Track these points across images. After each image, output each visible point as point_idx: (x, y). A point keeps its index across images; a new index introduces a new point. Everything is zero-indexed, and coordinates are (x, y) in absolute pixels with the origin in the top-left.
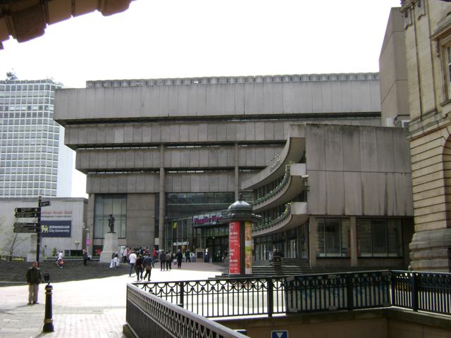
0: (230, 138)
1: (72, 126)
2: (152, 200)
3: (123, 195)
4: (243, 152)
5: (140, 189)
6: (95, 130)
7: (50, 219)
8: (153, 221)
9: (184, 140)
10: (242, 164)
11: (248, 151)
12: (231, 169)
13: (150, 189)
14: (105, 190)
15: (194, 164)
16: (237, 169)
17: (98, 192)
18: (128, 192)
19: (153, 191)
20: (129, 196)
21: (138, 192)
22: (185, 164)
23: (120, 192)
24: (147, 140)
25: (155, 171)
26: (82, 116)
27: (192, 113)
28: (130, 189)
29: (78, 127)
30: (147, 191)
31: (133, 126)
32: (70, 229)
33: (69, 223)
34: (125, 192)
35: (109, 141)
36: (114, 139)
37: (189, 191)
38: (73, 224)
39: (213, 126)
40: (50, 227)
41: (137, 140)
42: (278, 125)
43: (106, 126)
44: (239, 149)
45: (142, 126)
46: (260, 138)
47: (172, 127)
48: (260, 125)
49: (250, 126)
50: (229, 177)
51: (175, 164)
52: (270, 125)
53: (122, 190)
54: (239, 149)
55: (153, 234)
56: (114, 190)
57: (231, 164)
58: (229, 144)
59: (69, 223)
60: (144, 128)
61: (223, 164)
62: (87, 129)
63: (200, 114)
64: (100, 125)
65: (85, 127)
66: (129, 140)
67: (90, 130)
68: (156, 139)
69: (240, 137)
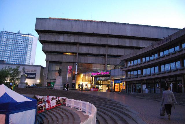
0: (105, 43)
4: (109, 49)
7: (28, 72)
9: (87, 42)
10: (109, 54)
12: (104, 56)
14: (53, 60)
15: (90, 52)
16: (107, 56)
17: (50, 60)
19: (73, 62)
20: (63, 63)
22: (87, 52)
24: (72, 41)
26: (47, 29)
27: (92, 32)
28: (64, 60)
30: (70, 61)
31: (67, 35)
32: (35, 76)
33: (35, 74)
34: (62, 61)
35: (57, 40)
37: (87, 63)
38: (37, 74)
39: (99, 38)
40: (28, 75)
41: (69, 40)
42: (123, 40)
45: (71, 35)
46: (117, 44)
47: (83, 37)
48: (117, 39)
49: (113, 39)
52: (120, 40)
53: (60, 60)
56: (57, 60)
57: (105, 53)
58: (103, 46)
59: (35, 74)
61: (102, 53)
62: (48, 35)
63: (95, 32)
65: (47, 34)
66: (65, 40)
67: (49, 35)
68: (76, 41)
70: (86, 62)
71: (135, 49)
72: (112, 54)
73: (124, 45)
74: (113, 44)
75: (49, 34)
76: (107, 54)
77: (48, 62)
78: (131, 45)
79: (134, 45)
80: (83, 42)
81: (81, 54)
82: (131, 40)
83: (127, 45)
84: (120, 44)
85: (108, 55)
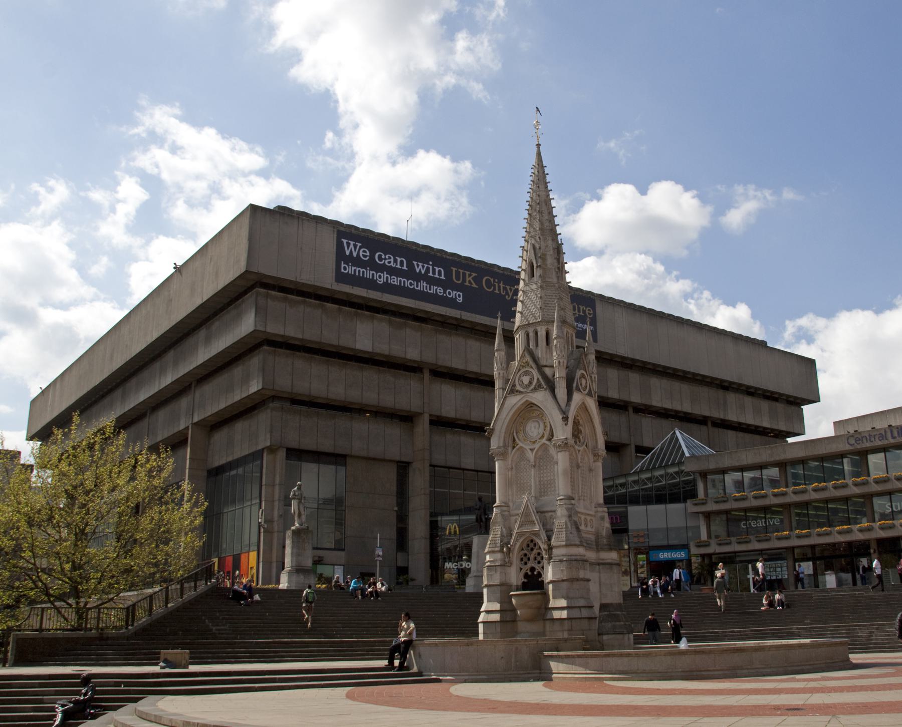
1: (273, 293)
2: (390, 475)
3: (337, 458)
8: (393, 519)
13: (395, 453)
14: (308, 443)
17: (294, 445)
19: (398, 459)
20: (349, 460)
23: (337, 452)
24: (413, 354)
25: (407, 419)
28: (357, 447)
35: (345, 341)
51: (448, 411)
55: (394, 546)
56: (326, 446)
68: (429, 357)
70: (452, 461)
77: (282, 454)
78: (625, 397)
80: (457, 363)
81: (440, 423)
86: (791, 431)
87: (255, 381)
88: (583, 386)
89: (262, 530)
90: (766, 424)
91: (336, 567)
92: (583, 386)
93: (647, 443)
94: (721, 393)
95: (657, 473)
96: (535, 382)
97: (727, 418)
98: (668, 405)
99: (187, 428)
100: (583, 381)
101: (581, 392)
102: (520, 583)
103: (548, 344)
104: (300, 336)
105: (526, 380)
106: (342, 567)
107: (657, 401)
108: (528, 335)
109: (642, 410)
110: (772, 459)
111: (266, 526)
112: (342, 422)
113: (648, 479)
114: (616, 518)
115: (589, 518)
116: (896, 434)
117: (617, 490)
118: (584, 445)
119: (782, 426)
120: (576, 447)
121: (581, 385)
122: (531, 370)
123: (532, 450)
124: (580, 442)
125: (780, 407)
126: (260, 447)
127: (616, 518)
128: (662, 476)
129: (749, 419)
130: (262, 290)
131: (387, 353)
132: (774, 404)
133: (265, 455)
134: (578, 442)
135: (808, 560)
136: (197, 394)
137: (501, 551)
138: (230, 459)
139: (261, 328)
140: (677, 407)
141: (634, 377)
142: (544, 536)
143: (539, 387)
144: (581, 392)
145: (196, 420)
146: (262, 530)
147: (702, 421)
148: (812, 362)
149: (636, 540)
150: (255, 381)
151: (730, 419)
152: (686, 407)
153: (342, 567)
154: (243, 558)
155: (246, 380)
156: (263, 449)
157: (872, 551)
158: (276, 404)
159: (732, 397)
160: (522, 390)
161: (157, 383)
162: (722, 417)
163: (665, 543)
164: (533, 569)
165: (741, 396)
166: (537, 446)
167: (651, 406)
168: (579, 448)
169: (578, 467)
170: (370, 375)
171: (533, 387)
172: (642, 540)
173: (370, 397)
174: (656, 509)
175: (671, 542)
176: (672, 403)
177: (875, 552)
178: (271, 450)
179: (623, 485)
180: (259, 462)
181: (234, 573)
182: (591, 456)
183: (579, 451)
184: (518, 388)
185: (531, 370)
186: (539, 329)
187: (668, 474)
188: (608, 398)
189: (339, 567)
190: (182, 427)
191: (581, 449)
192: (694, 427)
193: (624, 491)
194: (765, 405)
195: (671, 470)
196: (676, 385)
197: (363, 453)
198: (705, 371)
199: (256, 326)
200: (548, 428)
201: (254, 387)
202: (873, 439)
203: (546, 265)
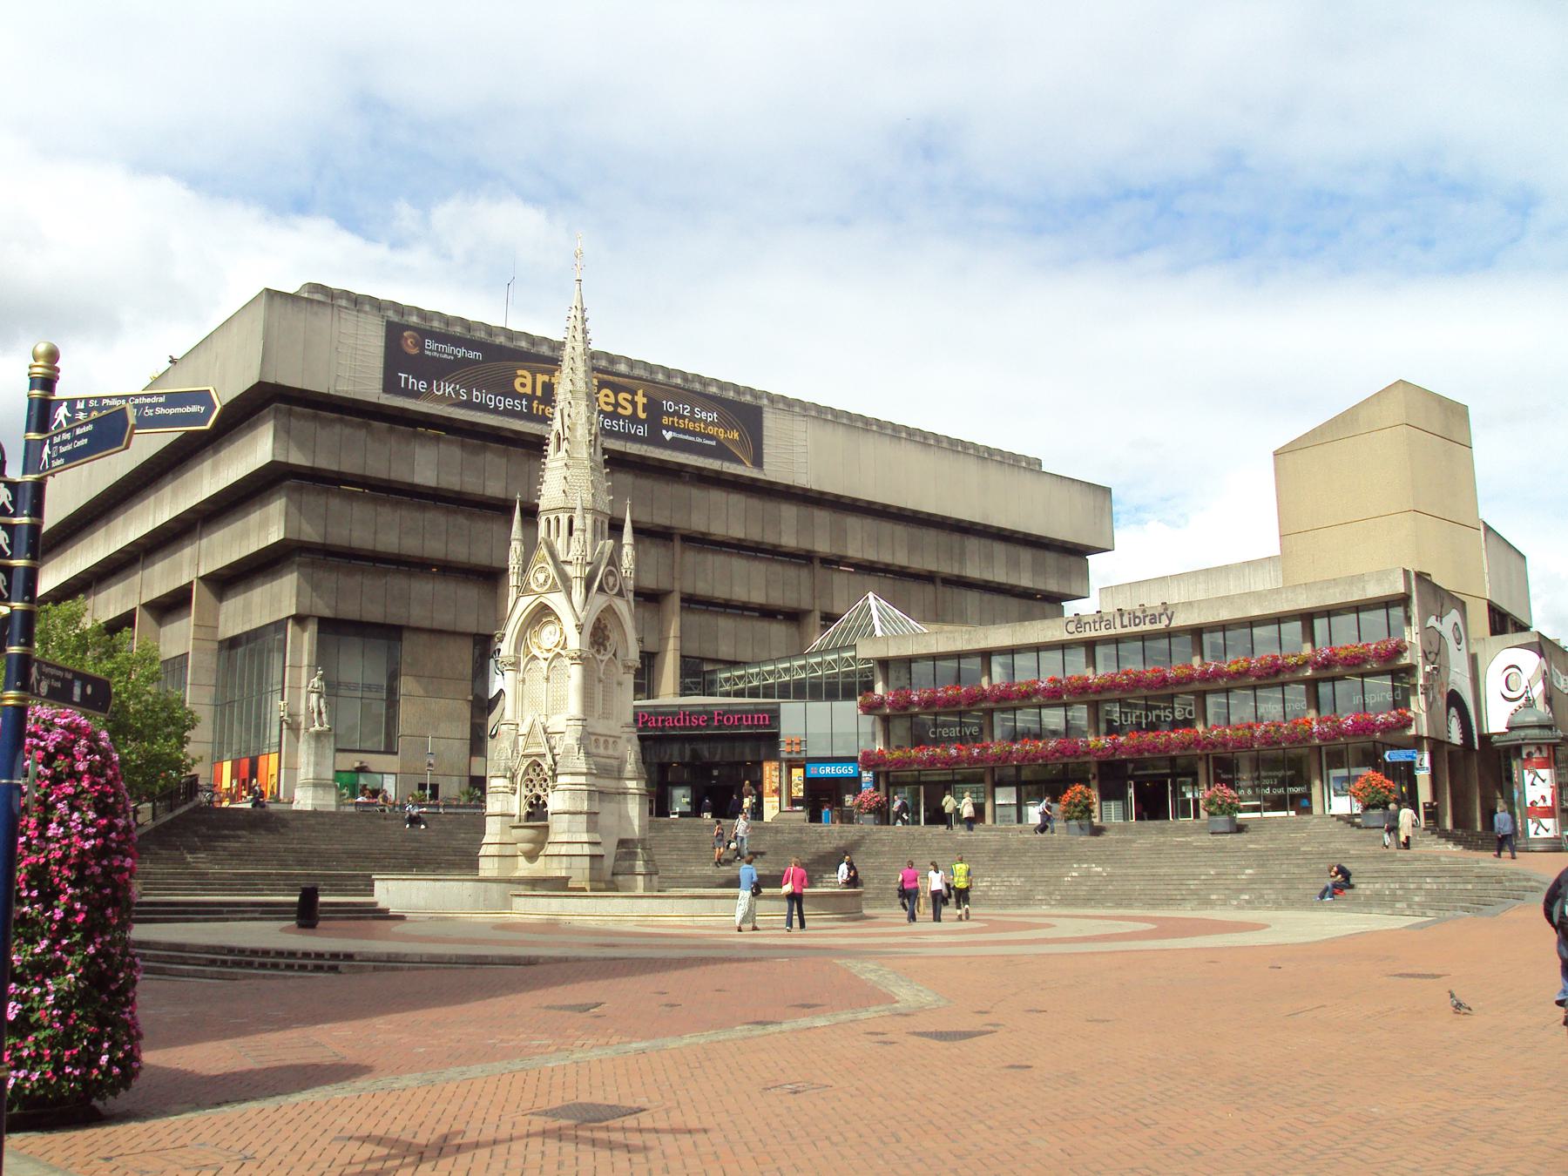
1: (298, 409)
4: (691, 557)
5: (443, 619)
6: (362, 433)
10: (689, 589)
11: (700, 557)
13: (469, 623)
16: (675, 602)
17: (327, 613)
18: (413, 623)
19: (474, 630)
20: (406, 635)
21: (436, 625)
28: (417, 615)
29: (315, 418)
30: (461, 627)
31: (463, 446)
34: (403, 622)
35: (399, 473)
36: (413, 471)
43: (391, 430)
44: (683, 552)
46: (737, 532)
48: (738, 501)
49: (717, 496)
50: (646, 615)
52: (755, 504)
53: (396, 615)
54: (683, 552)
57: (664, 584)
60: (489, 456)
62: (338, 428)
64: (376, 424)
65: (333, 421)
66: (452, 481)
67: (348, 431)
69: (698, 523)
71: (817, 564)
72: (702, 588)
73: (770, 538)
74: (718, 529)
75: (346, 424)
76: (677, 587)
77: (312, 628)
78: (805, 544)
79: (823, 547)
82: (805, 511)
83: (789, 541)
84: (754, 534)
85: (692, 602)
86: (1067, 592)
87: (276, 527)
88: (611, 584)
89: (285, 726)
90: (1026, 581)
91: (385, 776)
92: (611, 584)
93: (836, 610)
94: (956, 537)
95: (829, 658)
96: (550, 581)
97: (964, 574)
98: (871, 555)
99: (191, 583)
100: (611, 579)
101: (605, 592)
102: (523, 813)
103: (571, 533)
104: (335, 467)
105: (541, 577)
106: (394, 777)
107: (855, 551)
108: (549, 522)
109: (831, 562)
110: (970, 648)
111: (290, 721)
112: (398, 583)
113: (819, 664)
114: (764, 718)
115: (611, 740)
116: (1126, 622)
117: (780, 677)
118: (611, 655)
119: (1053, 586)
120: (599, 657)
121: (607, 584)
122: (547, 566)
123: (546, 659)
124: (605, 650)
125: (1050, 558)
126: (284, 615)
127: (764, 718)
128: (834, 661)
129: (1000, 575)
130: (282, 406)
131: (457, 488)
132: (1040, 553)
133: (290, 626)
134: (602, 651)
135: (1009, 784)
136: (204, 542)
137: (505, 777)
138: (247, 628)
139: (281, 459)
140: (886, 557)
141: (822, 516)
142: (549, 757)
143: (553, 589)
144: (605, 592)
145: (202, 573)
146: (285, 726)
147: (928, 578)
148: (1106, 491)
149: (788, 748)
150: (276, 527)
151: (968, 575)
152: (901, 559)
153: (394, 777)
154: (262, 761)
155: (264, 525)
156: (288, 618)
157: (1090, 776)
158: (306, 558)
159: (973, 544)
160: (539, 590)
161: (151, 518)
162: (956, 571)
163: (828, 754)
164: (538, 797)
165: (988, 542)
166: (551, 655)
167: (846, 557)
168: (603, 658)
169: (600, 681)
170: (435, 519)
171: (547, 586)
172: (796, 748)
173: (434, 547)
174: (819, 708)
175: (838, 753)
176: (878, 553)
177: (1094, 778)
178: (299, 619)
179: (787, 670)
180: (280, 636)
181: (251, 781)
182: (621, 670)
183: (602, 661)
184: (533, 586)
185: (547, 566)
186: (561, 516)
187: (843, 659)
188: (780, 546)
189: (390, 776)
190: (185, 581)
191: (606, 658)
192: (914, 588)
193: (787, 678)
194: (1026, 555)
195: (847, 655)
196: (887, 527)
197: (426, 624)
198: (929, 506)
199: (274, 455)
200: (563, 637)
201: (275, 535)
202: (1097, 627)
203: (575, 437)
